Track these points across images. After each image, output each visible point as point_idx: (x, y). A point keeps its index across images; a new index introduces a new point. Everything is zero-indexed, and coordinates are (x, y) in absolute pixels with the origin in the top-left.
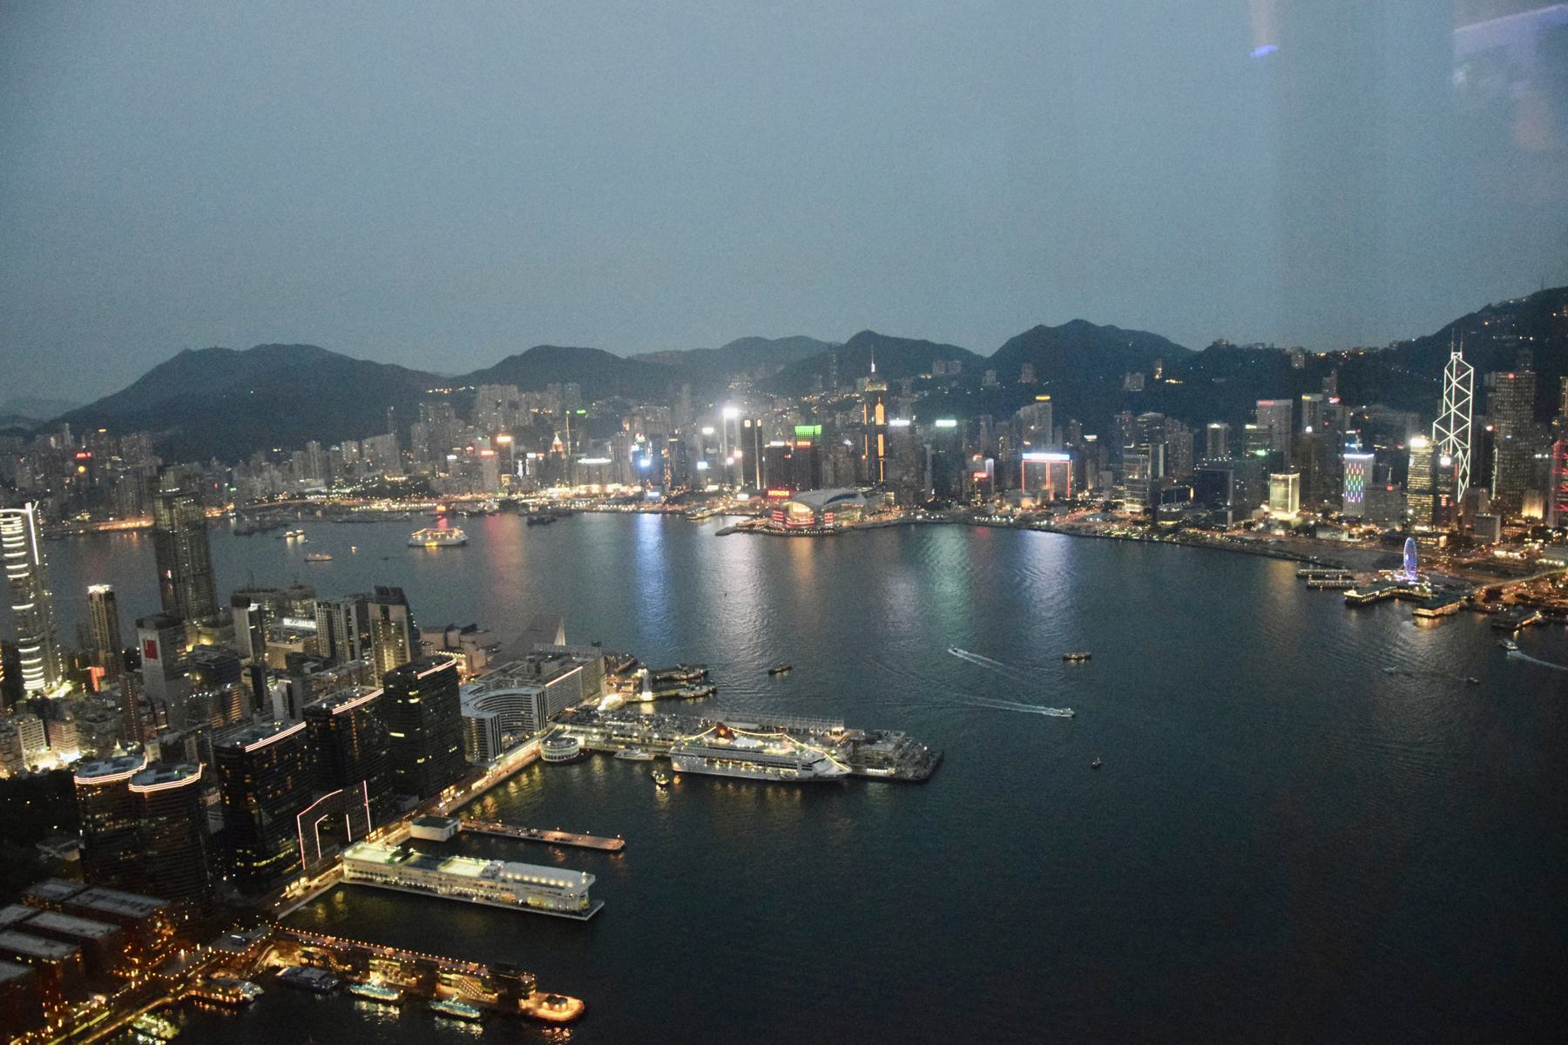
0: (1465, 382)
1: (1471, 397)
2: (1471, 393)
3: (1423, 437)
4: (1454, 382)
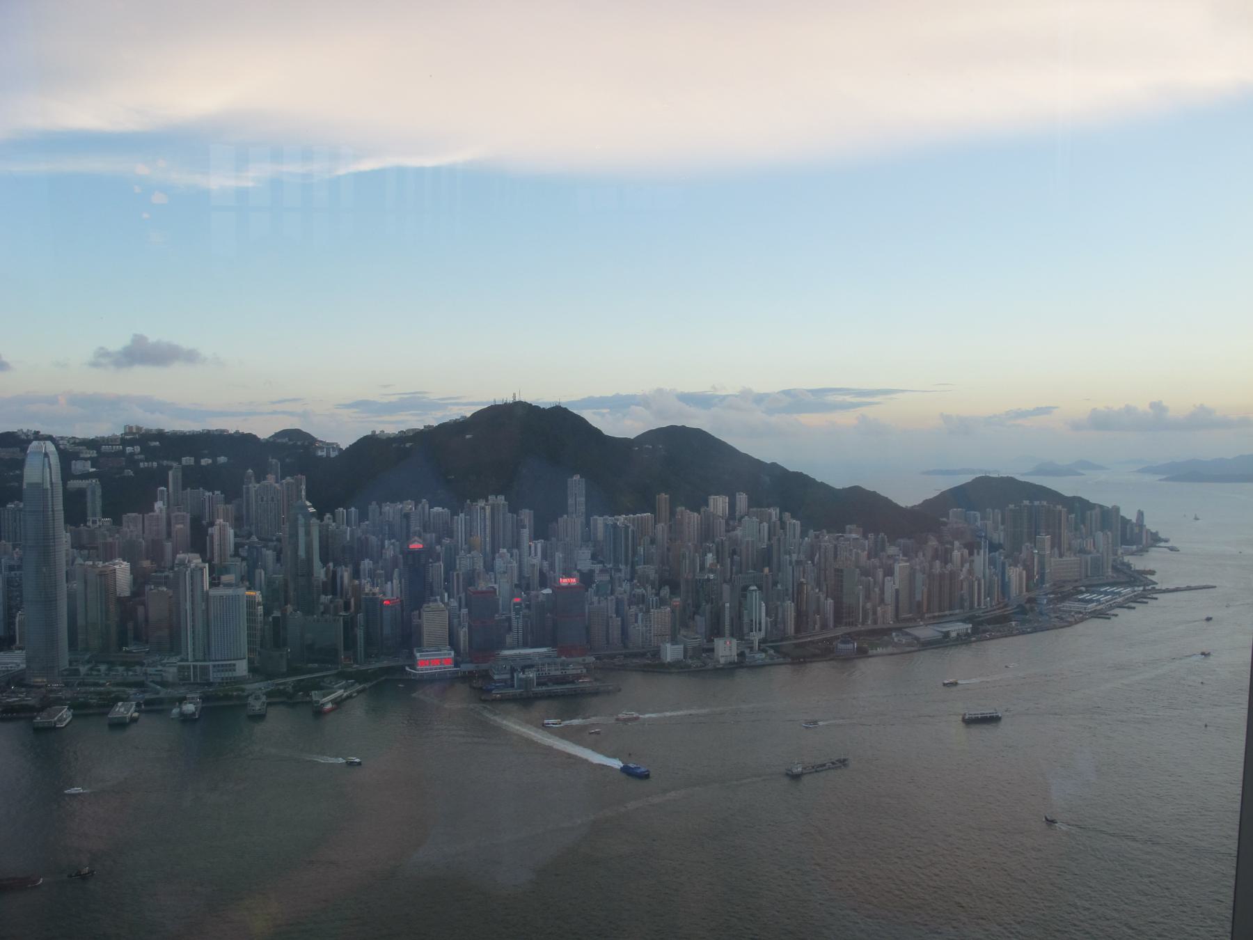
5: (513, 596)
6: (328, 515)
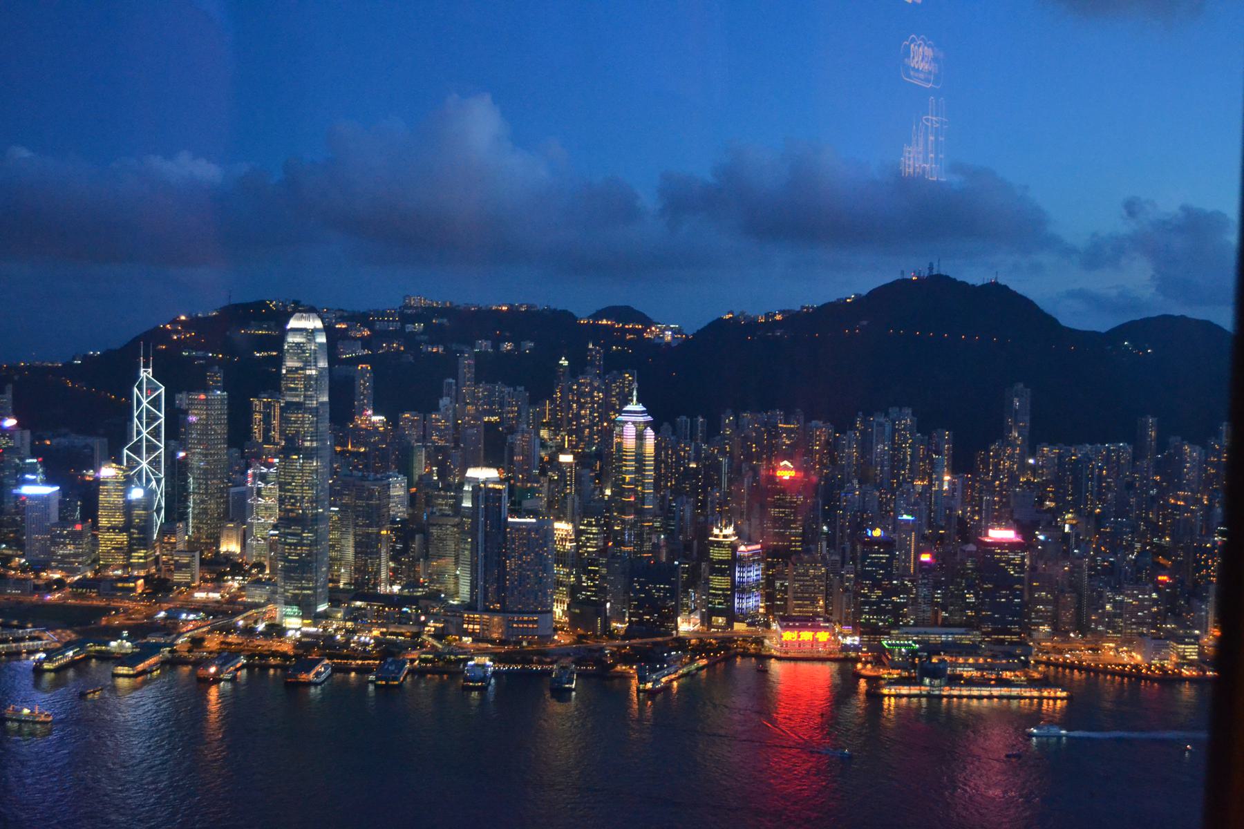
0: (155, 403)
1: (163, 420)
2: (162, 416)
3: (114, 465)
4: (145, 403)
5: (919, 552)
6: (666, 425)
